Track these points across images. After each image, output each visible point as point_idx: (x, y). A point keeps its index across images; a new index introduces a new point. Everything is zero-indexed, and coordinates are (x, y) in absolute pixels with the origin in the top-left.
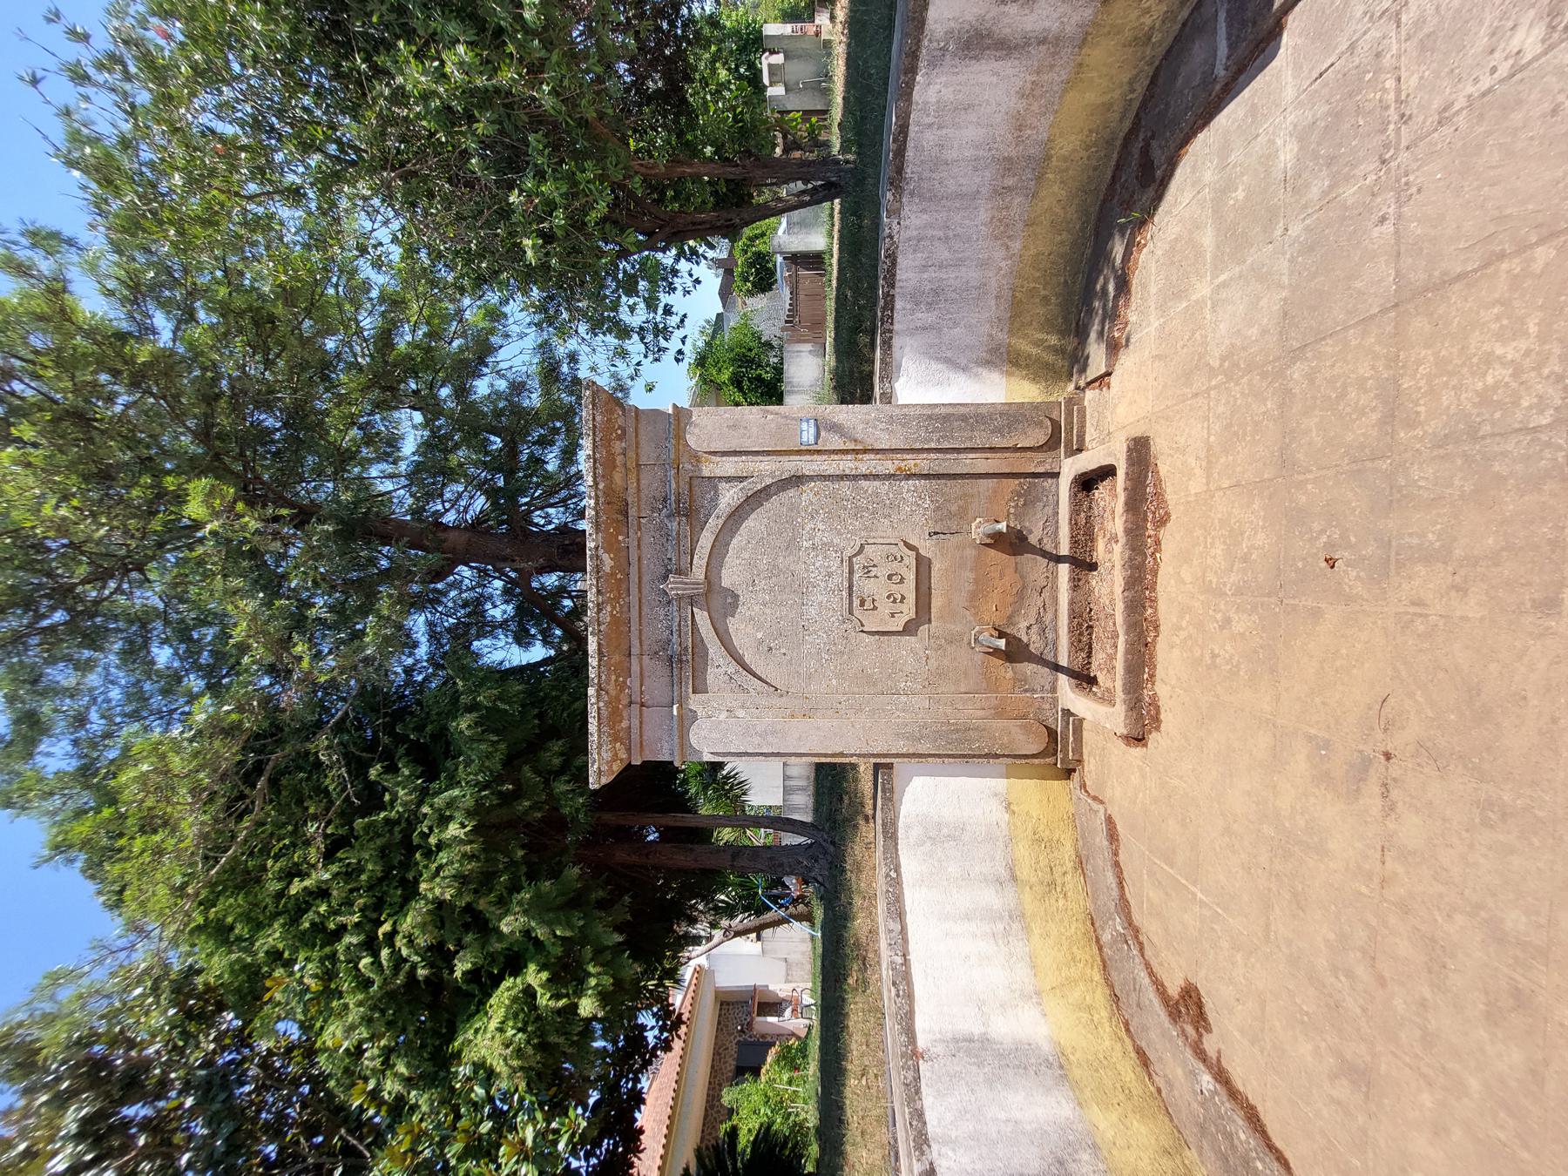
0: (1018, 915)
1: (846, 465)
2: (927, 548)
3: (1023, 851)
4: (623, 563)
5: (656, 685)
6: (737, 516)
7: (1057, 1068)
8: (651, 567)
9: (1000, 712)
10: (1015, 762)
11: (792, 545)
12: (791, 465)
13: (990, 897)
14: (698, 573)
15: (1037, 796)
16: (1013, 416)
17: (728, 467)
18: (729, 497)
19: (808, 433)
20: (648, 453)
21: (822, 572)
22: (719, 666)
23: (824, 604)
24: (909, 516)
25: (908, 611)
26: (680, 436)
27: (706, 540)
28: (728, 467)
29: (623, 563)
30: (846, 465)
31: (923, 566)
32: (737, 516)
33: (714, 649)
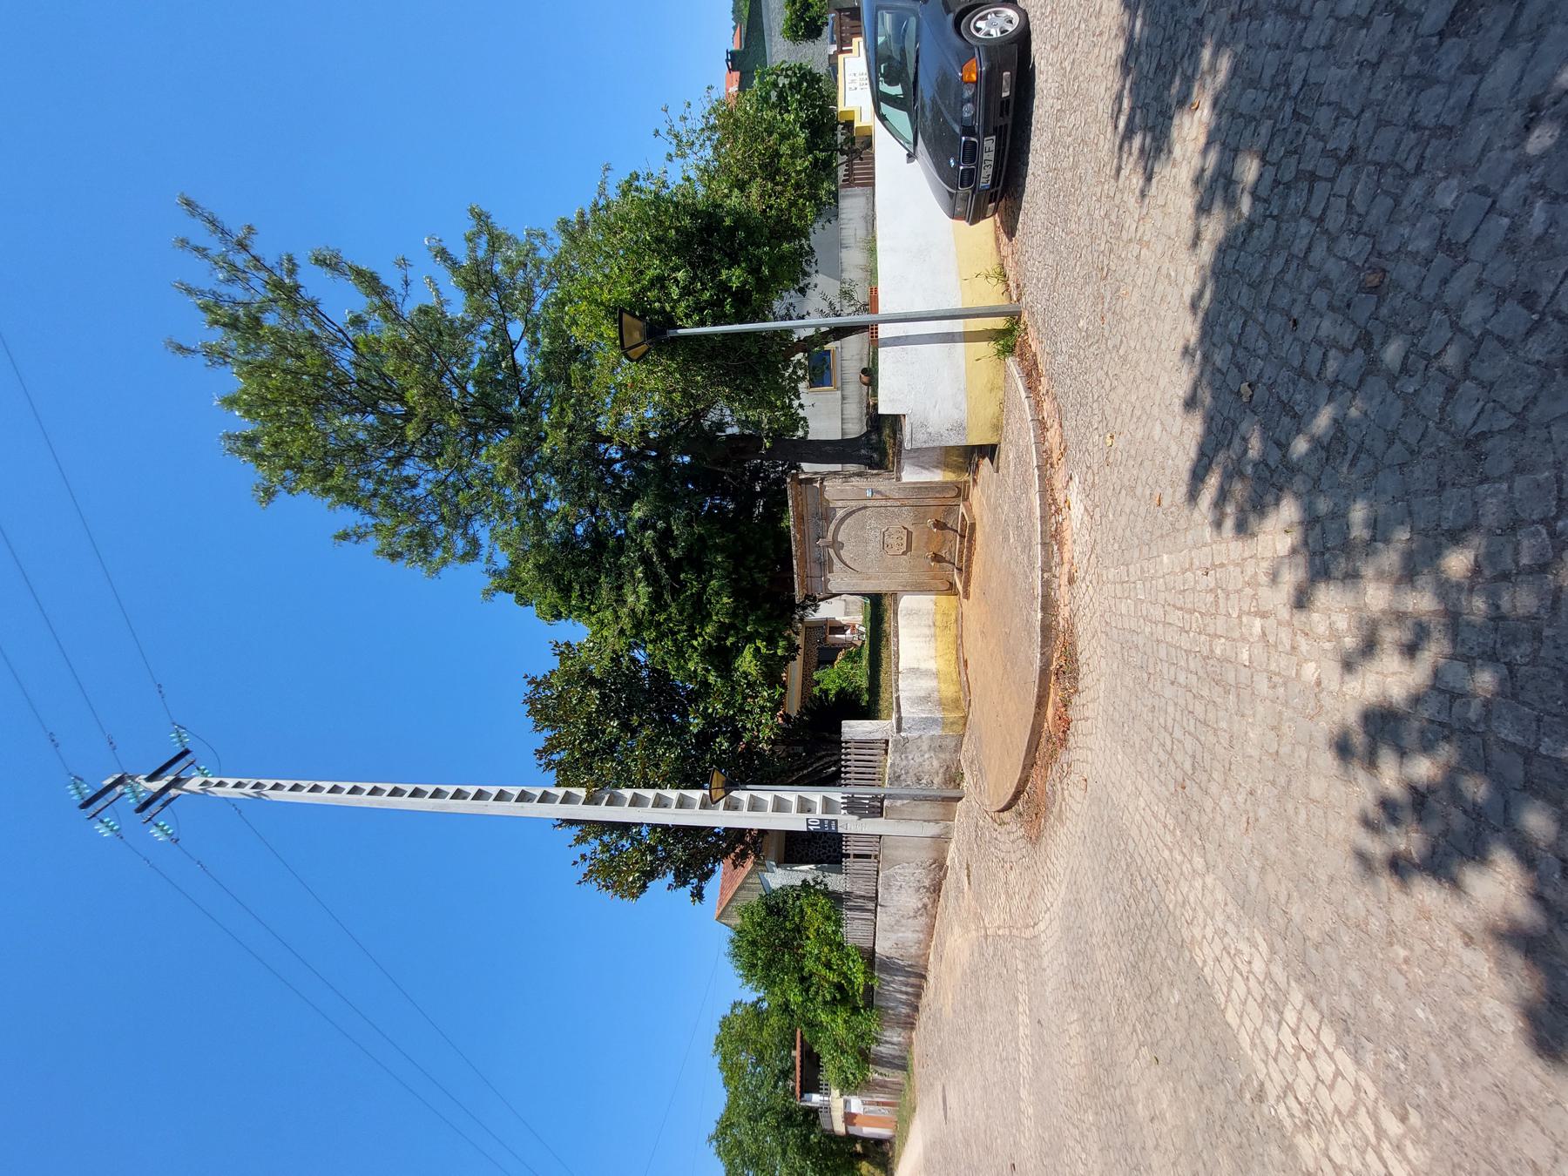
0: (934, 636)
1: (883, 503)
2: (911, 528)
3: (938, 617)
4: (803, 536)
5: (816, 571)
6: (843, 520)
7: (936, 675)
8: (813, 536)
9: (934, 578)
10: (938, 592)
11: (863, 528)
12: (862, 503)
13: (926, 631)
14: (830, 537)
15: (944, 600)
16: (943, 486)
17: (840, 504)
18: (840, 514)
19: (869, 494)
20: (810, 500)
21: (874, 536)
22: (837, 565)
23: (874, 546)
24: (906, 518)
25: (904, 548)
26: (822, 494)
27: (832, 527)
28: (840, 504)
29: (803, 536)
30: (883, 503)
31: (909, 534)
32: (843, 520)
33: (836, 560)
